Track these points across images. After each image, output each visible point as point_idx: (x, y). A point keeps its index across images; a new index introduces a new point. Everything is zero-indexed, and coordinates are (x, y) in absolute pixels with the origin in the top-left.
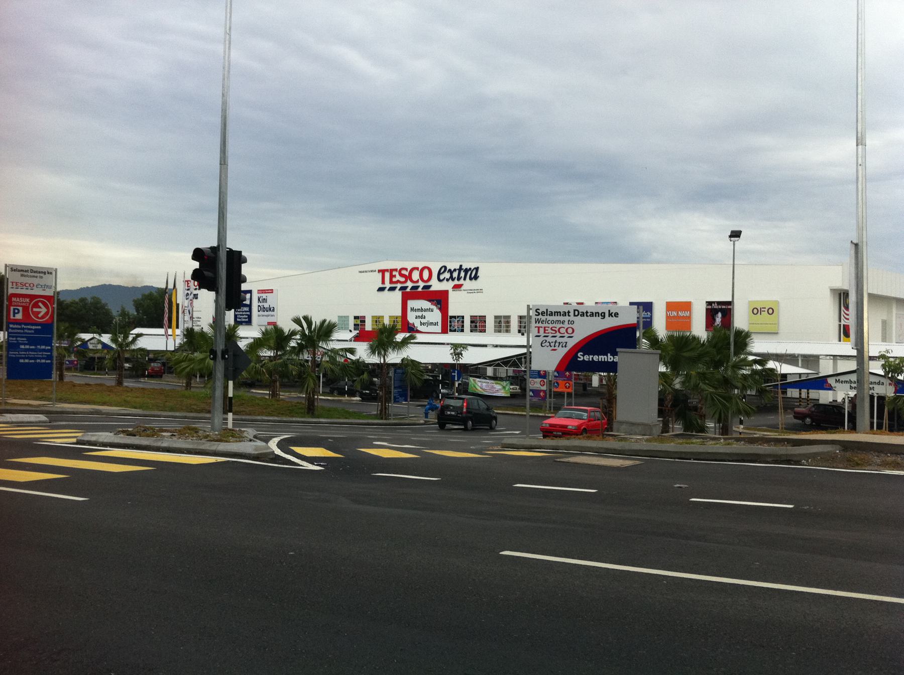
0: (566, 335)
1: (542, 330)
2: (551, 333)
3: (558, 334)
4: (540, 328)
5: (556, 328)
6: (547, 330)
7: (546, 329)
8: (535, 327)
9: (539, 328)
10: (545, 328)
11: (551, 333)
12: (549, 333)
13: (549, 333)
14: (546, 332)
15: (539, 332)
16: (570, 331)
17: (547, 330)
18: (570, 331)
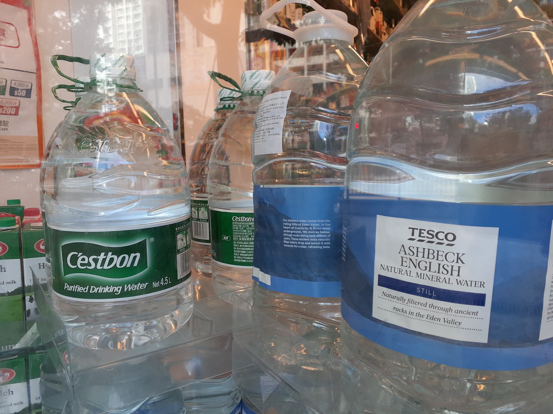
0: (445, 241)
1: (417, 232)
2: (427, 237)
3: (435, 239)
4: (415, 230)
5: (434, 231)
6: (423, 233)
7: (422, 231)
8: (410, 228)
9: (413, 229)
10: (421, 230)
11: (427, 237)
12: (424, 237)
13: (424, 237)
14: (422, 235)
15: (413, 235)
16: (450, 237)
17: (423, 233)
18: (450, 237)
